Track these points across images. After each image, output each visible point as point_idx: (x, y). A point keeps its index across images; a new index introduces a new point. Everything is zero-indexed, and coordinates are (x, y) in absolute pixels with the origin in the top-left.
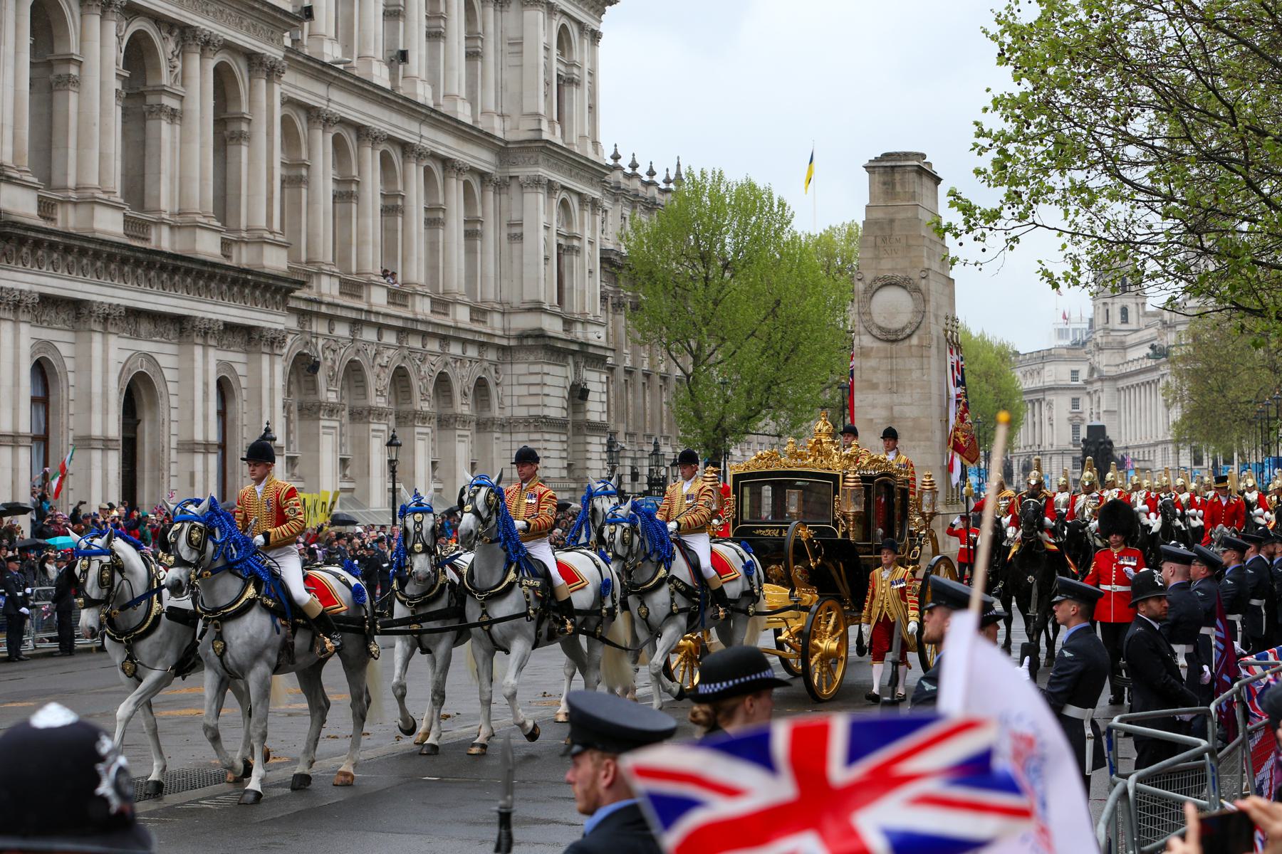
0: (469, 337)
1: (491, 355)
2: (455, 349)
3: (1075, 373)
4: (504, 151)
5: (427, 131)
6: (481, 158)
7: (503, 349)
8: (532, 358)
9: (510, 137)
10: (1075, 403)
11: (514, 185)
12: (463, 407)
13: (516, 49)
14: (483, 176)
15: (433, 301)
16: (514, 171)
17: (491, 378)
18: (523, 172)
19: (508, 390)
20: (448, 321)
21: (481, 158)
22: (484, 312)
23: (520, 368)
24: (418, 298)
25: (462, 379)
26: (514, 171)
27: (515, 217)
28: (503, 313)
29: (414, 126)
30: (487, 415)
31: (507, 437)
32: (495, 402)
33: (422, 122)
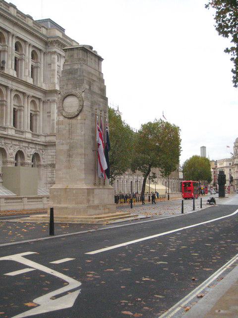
0: (30, 141)
1: (41, 147)
2: (24, 144)
3: (230, 164)
4: (45, 92)
5: (14, 84)
6: (39, 95)
7: (45, 146)
8: (52, 148)
9: (47, 89)
10: (230, 170)
11: (49, 103)
12: (28, 160)
13: (50, 66)
14: (39, 99)
15: (15, 130)
16: (49, 98)
17: (40, 153)
18: (51, 98)
19: (46, 157)
20: (24, 136)
21: (39, 95)
22: (38, 136)
23: (49, 151)
24: (9, 130)
25: (29, 152)
26: (49, 98)
27: (48, 111)
28: (45, 136)
29: (10, 82)
30: (39, 163)
31: (46, 169)
32: (41, 159)
33: (12, 81)
